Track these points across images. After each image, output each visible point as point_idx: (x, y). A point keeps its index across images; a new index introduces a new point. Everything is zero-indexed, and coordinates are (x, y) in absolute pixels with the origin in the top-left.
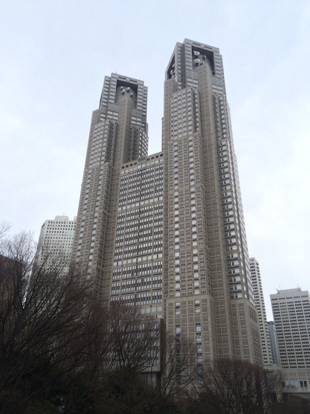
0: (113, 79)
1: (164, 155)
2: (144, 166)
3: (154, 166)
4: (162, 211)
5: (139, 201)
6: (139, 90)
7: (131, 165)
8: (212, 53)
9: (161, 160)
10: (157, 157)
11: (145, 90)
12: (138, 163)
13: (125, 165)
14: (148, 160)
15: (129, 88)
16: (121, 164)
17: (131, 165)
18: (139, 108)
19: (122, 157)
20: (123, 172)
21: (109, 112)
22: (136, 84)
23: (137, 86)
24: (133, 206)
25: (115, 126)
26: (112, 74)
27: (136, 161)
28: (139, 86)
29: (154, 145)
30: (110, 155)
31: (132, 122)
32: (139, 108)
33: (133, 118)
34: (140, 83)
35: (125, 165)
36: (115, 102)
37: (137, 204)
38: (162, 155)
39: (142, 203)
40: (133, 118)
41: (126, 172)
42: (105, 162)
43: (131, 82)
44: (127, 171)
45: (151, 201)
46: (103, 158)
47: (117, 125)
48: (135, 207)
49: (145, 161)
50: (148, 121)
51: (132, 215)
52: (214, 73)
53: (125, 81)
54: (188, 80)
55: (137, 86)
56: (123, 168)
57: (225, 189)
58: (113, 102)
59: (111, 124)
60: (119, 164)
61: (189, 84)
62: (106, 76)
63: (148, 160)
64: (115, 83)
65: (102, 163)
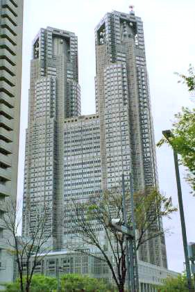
2: (83, 124)
6: (71, 42)
7: (73, 121)
8: (136, 23)
14: (87, 119)
15: (62, 40)
24: (77, 157)
25: (54, 80)
28: (71, 38)
29: (88, 105)
30: (54, 112)
33: (68, 72)
35: (67, 120)
37: (80, 156)
38: (98, 117)
40: (68, 72)
41: (67, 126)
45: (91, 155)
54: (118, 54)
61: (118, 58)
63: (87, 119)
64: (51, 37)
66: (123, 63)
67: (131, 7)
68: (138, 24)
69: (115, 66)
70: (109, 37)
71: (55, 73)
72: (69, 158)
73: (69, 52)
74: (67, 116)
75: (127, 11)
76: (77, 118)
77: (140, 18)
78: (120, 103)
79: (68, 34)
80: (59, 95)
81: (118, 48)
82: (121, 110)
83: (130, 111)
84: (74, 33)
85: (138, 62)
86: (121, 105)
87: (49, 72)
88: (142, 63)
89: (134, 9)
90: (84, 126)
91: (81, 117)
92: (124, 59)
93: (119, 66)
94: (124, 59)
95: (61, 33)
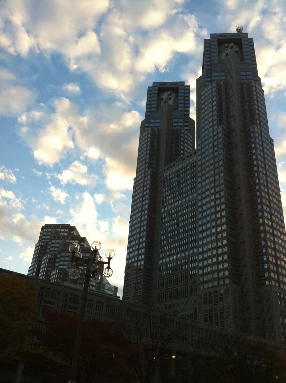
2: (181, 166)
5: (178, 201)
13: (166, 168)
14: (184, 159)
15: (169, 92)
17: (171, 167)
18: (180, 109)
21: (152, 121)
22: (176, 86)
23: (177, 88)
27: (175, 162)
31: (174, 124)
32: (180, 109)
33: (174, 120)
34: (181, 84)
36: (157, 109)
37: (176, 204)
39: (180, 202)
40: (174, 120)
42: (148, 169)
43: (171, 86)
44: (168, 174)
45: (187, 199)
46: (147, 165)
48: (175, 206)
49: (181, 161)
51: (172, 214)
52: (243, 60)
53: (165, 86)
55: (177, 88)
56: (165, 171)
58: (155, 109)
62: (149, 87)
64: (156, 92)
65: (147, 169)
71: (159, 125)
72: (166, 209)
86: (215, 127)
92: (224, 78)
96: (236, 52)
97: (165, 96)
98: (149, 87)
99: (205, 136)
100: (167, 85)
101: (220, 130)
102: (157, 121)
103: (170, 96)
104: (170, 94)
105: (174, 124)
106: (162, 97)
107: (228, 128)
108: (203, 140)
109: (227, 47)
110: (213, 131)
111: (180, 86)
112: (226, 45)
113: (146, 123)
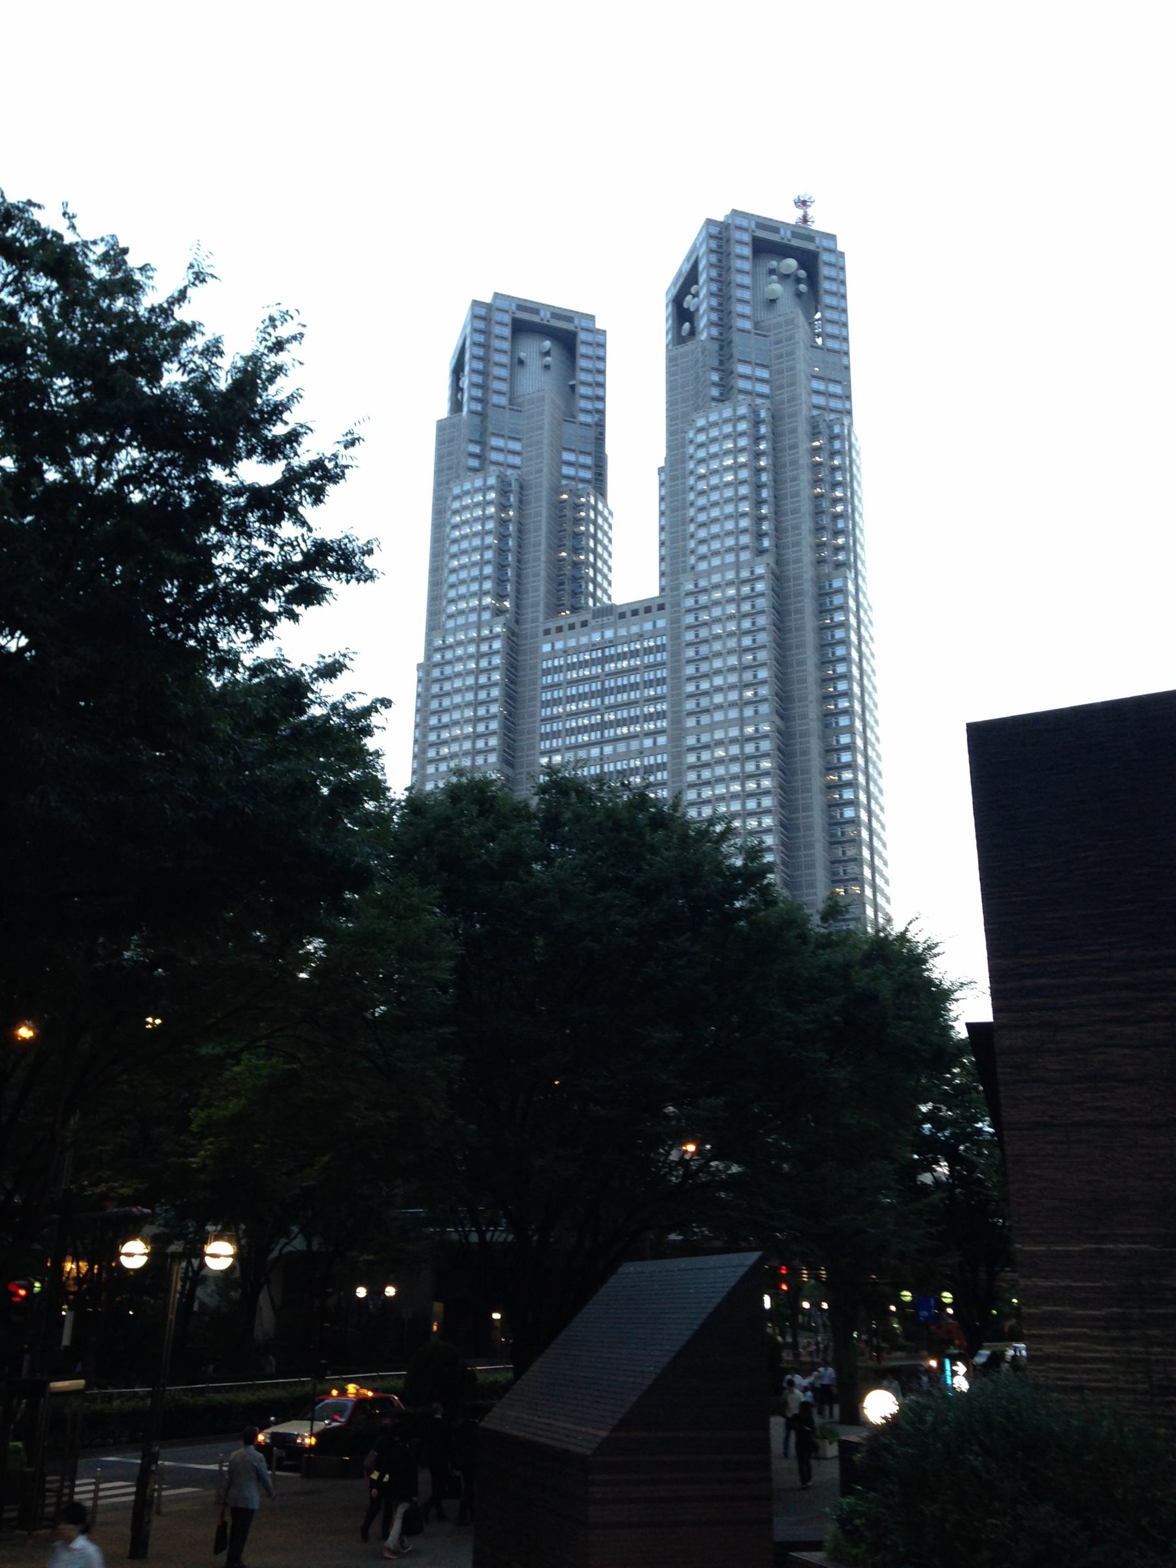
0: (498, 316)
1: (667, 607)
2: (609, 634)
3: (641, 637)
4: (665, 777)
6: (582, 349)
9: (661, 623)
10: (648, 610)
11: (599, 343)
12: (592, 623)
13: (552, 625)
15: (547, 344)
16: (541, 619)
18: (582, 418)
19: (542, 595)
20: (547, 648)
22: (570, 327)
25: (515, 486)
26: (496, 295)
28: (583, 336)
31: (566, 470)
32: (582, 418)
33: (568, 456)
34: (584, 324)
35: (552, 625)
38: (661, 607)
39: (608, 750)
40: (568, 456)
44: (559, 645)
45: (634, 745)
47: (521, 487)
49: (612, 618)
50: (608, 449)
54: (742, 369)
56: (547, 632)
57: (837, 723)
59: (503, 481)
60: (535, 620)
61: (743, 384)
62: (476, 303)
63: (622, 616)
64: (507, 332)
65: (486, 616)
66: (759, 401)
67: (804, 203)
68: (825, 257)
69: (727, 413)
70: (711, 324)
71: (516, 460)
73: (573, 388)
74: (555, 609)
75: (790, 216)
76: (587, 616)
77: (833, 237)
78: (737, 549)
79: (568, 316)
80: (531, 538)
81: (740, 345)
82: (745, 574)
83: (780, 580)
84: (592, 318)
85: (820, 400)
86: (745, 556)
87: (494, 456)
88: (834, 404)
89: (811, 212)
90: (612, 643)
91: (609, 610)
92: (765, 389)
93: (742, 410)
94: (765, 389)
95: (544, 317)
96: (799, 294)
97: (533, 349)
98: (476, 303)
99: (709, 573)
100: (542, 313)
101: (760, 570)
102: (512, 445)
103: (548, 359)
104: (547, 354)
105: (566, 470)
106: (522, 355)
107: (777, 563)
108: (703, 583)
109: (772, 272)
110: (738, 566)
111: (583, 329)
112: (774, 264)
113: (471, 441)
